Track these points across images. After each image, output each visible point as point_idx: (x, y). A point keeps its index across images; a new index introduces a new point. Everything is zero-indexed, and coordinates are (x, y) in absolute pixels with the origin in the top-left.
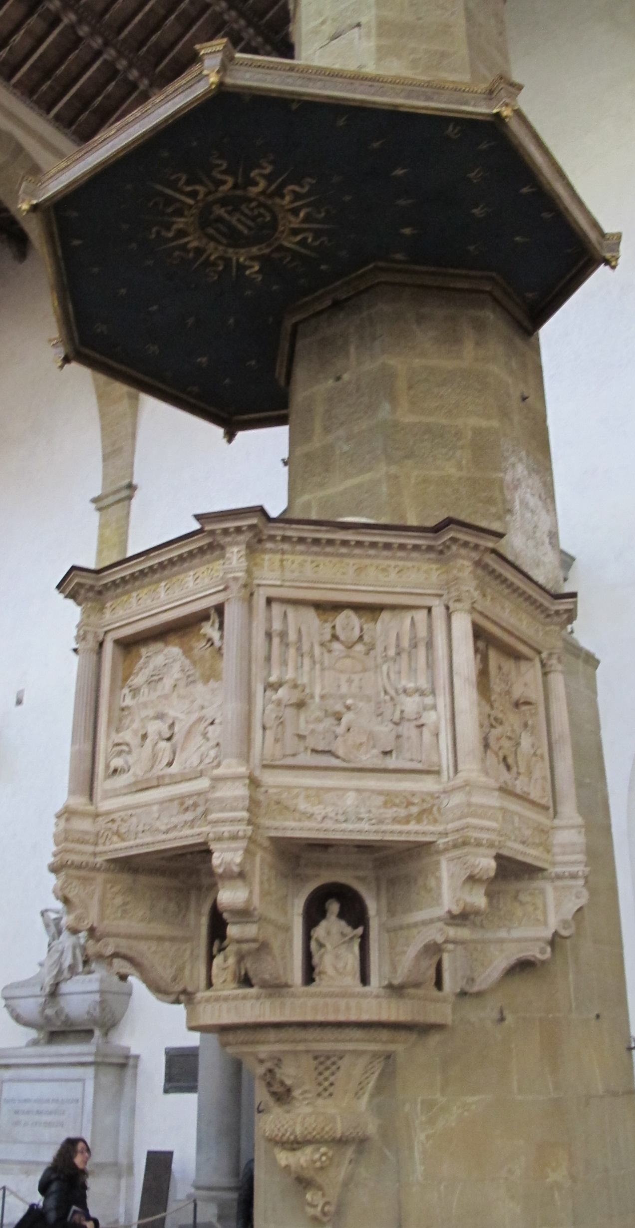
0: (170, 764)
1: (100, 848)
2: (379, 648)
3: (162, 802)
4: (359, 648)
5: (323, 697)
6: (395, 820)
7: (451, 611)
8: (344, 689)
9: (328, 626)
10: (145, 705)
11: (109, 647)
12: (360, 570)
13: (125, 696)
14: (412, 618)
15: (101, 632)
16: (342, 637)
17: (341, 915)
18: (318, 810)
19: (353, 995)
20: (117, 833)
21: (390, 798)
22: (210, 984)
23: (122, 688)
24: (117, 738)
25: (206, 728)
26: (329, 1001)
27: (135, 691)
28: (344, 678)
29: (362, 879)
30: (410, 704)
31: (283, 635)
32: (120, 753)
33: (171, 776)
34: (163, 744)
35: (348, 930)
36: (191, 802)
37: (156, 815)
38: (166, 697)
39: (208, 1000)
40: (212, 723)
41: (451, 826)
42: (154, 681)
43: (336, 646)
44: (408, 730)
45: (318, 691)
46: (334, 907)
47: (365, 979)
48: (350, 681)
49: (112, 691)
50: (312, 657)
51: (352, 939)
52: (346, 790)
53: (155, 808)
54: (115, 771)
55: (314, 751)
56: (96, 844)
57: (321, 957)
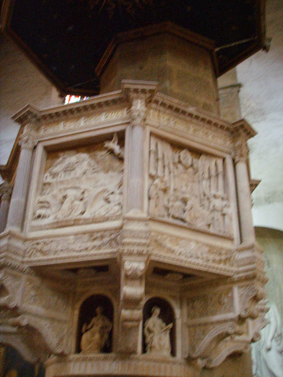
0: (83, 213)
1: (26, 259)
2: (200, 173)
3: (76, 234)
4: (190, 170)
5: (175, 190)
6: (214, 261)
7: (236, 161)
8: (184, 189)
9: (176, 156)
10: (62, 182)
11: (40, 150)
12: (195, 131)
13: (46, 177)
14: (216, 161)
15: (36, 141)
16: (184, 162)
17: (160, 316)
18: (176, 248)
19: (168, 362)
20: (41, 251)
21: (212, 249)
22: (78, 350)
23: (45, 173)
24: (42, 198)
25: (108, 195)
26: (157, 365)
27: (54, 175)
28: (184, 184)
29: (174, 297)
30: (218, 203)
31: (156, 153)
32: (42, 207)
33: (85, 220)
34: (77, 202)
35: (164, 325)
36: (99, 235)
37: (73, 241)
38: (78, 179)
39: (78, 360)
40: (112, 193)
41: (241, 269)
42: (68, 169)
43: (180, 166)
44: (217, 215)
45: (172, 187)
46: (157, 311)
47: (173, 353)
48: (187, 186)
49: (40, 173)
50: (169, 169)
51: (166, 330)
52: (190, 240)
53: (72, 237)
54: (39, 216)
55: (173, 217)
56: (24, 257)
57: (152, 338)
